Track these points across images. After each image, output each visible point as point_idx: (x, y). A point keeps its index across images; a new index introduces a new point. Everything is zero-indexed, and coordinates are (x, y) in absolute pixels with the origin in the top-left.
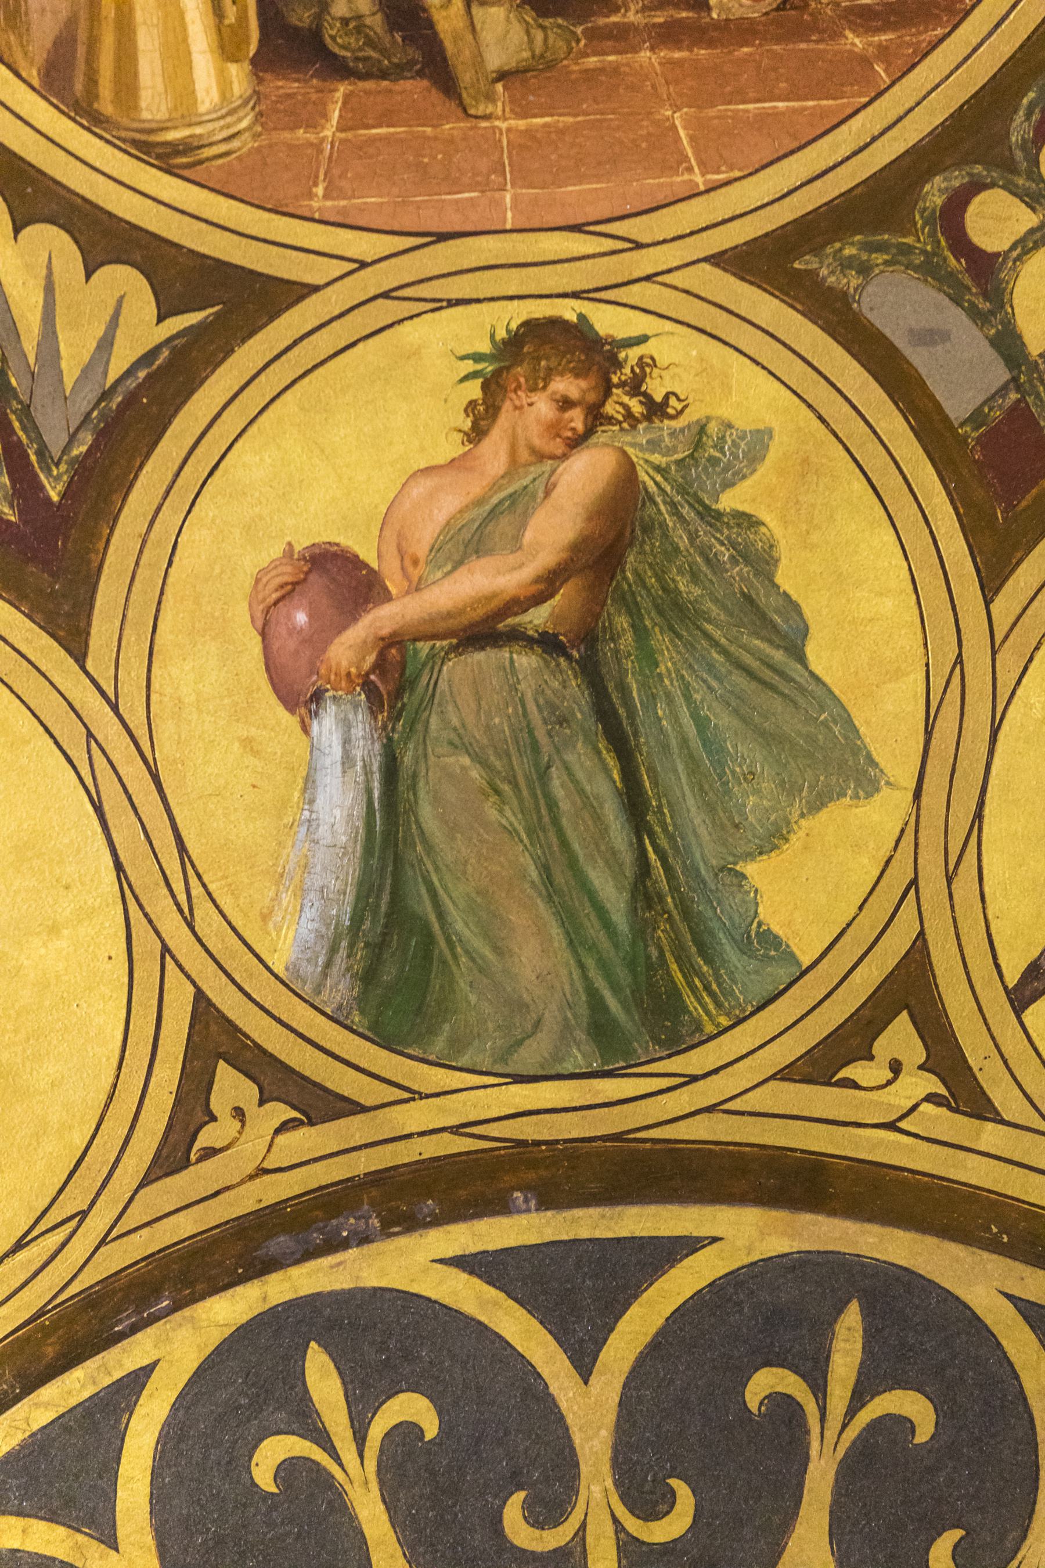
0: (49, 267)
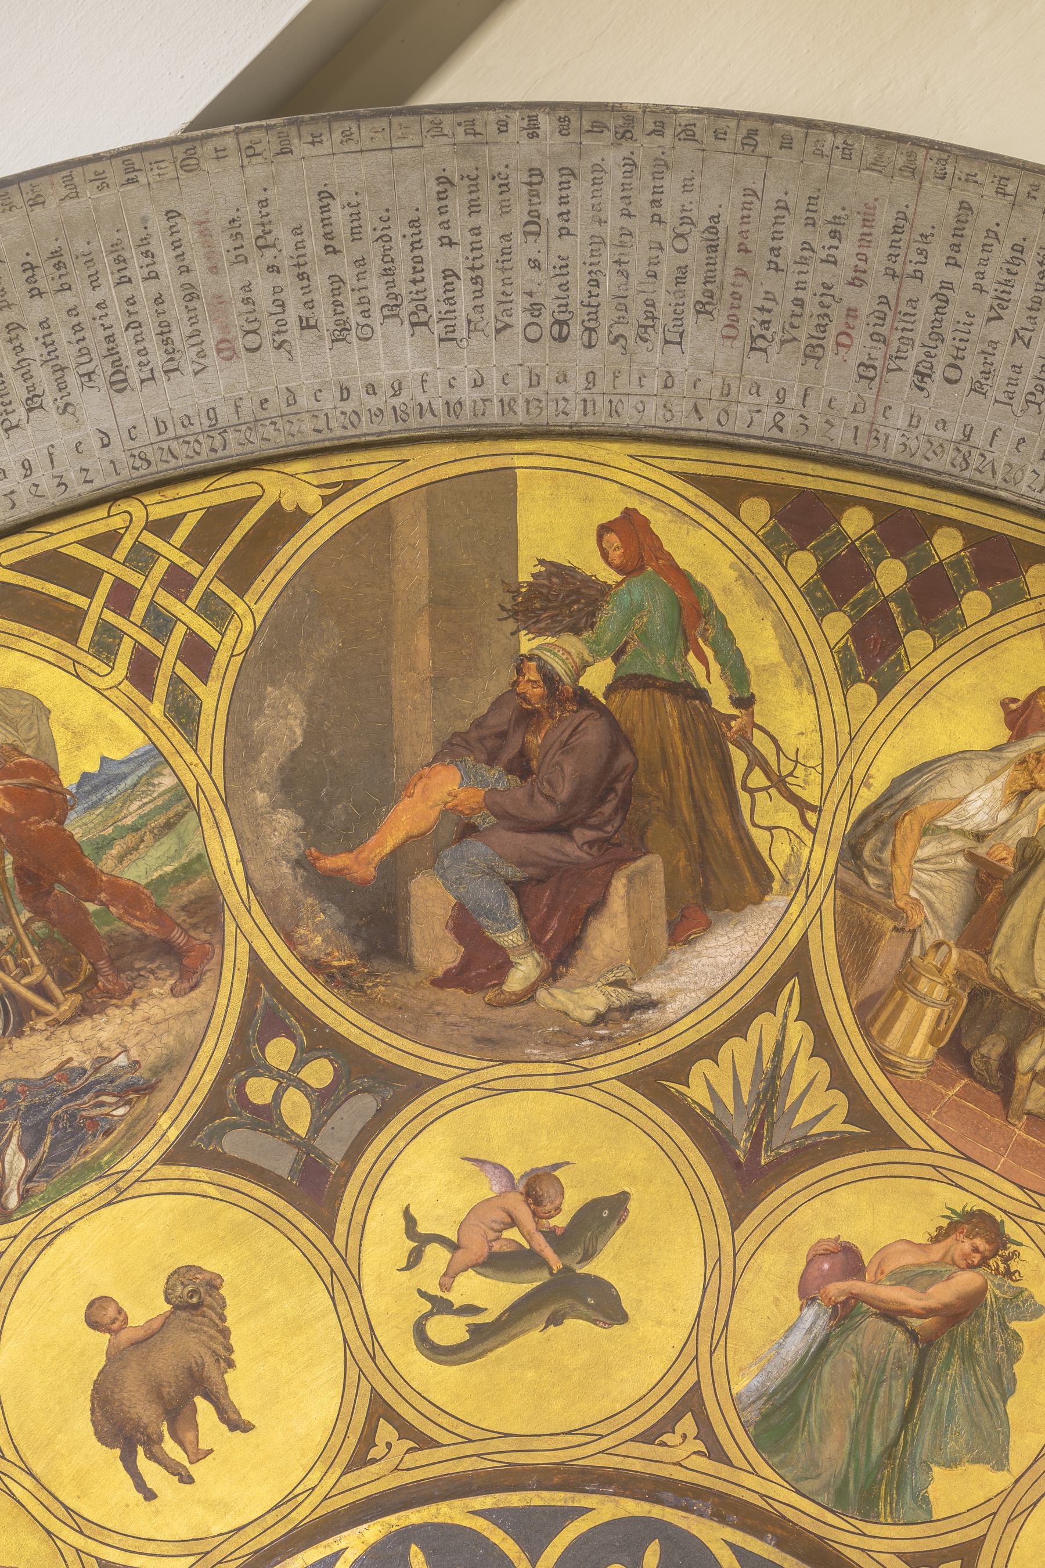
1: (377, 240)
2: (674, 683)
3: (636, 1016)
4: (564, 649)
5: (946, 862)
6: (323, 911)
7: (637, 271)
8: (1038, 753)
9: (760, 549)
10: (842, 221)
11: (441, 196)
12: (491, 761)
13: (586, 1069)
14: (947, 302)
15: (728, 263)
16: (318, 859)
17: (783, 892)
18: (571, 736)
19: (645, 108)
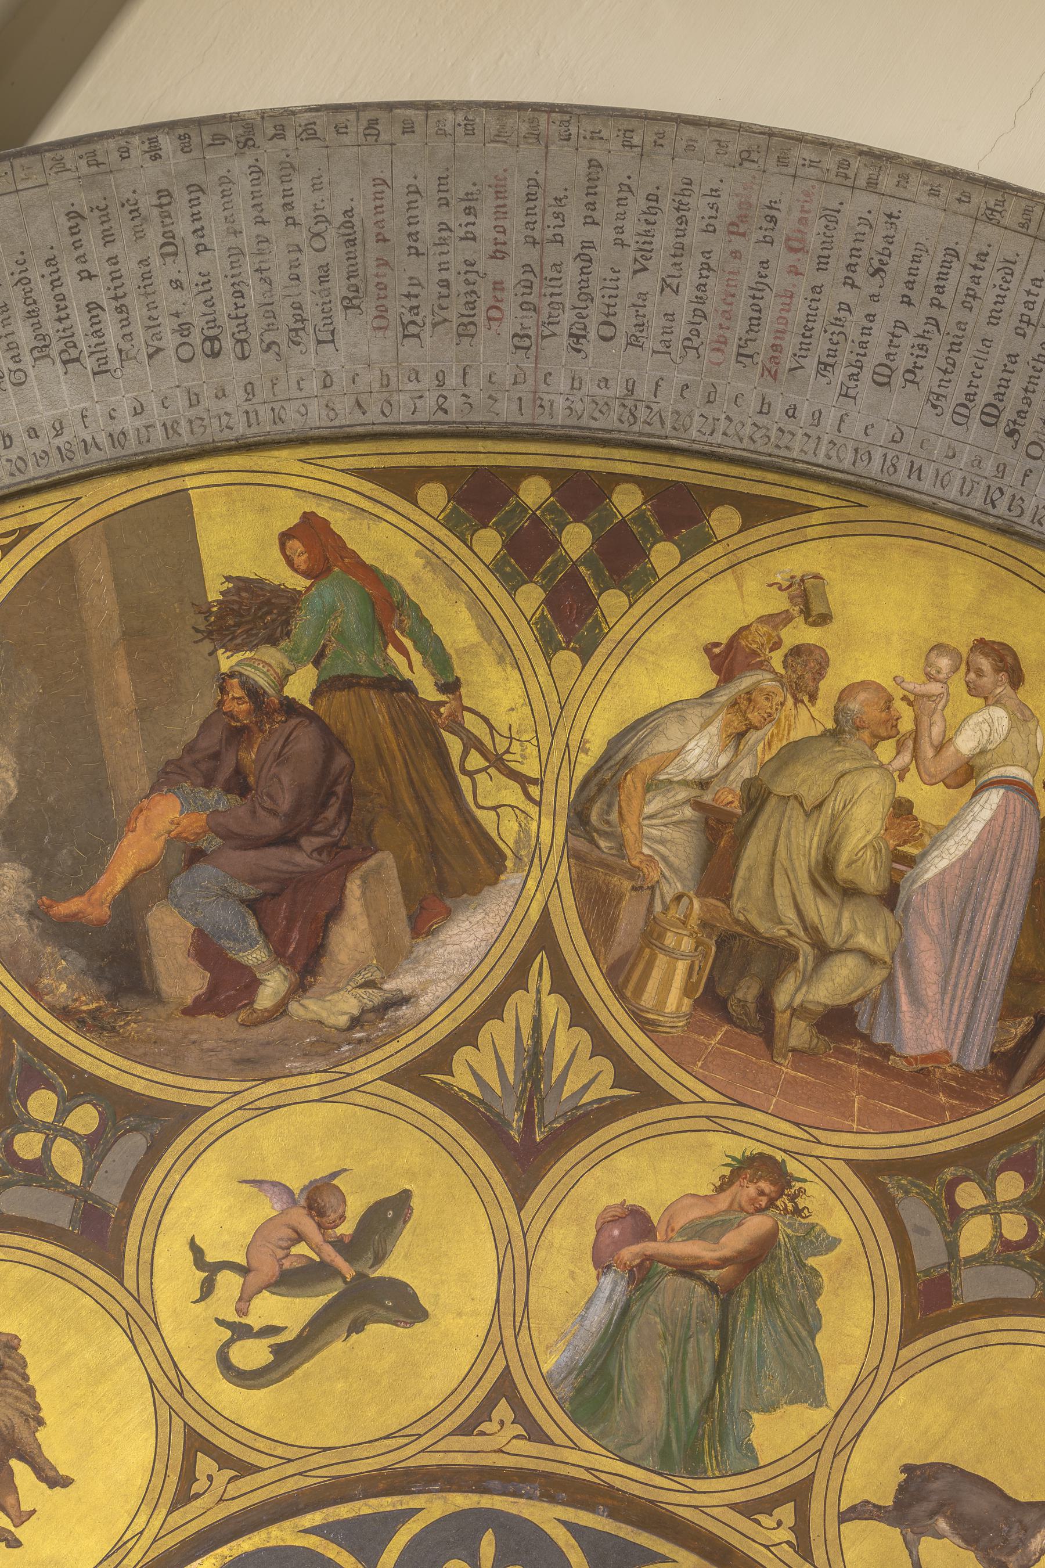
0: (577, 1047)
1: (16, 284)
2: (378, 679)
3: (391, 1014)
4: (263, 662)
5: (674, 815)
6: (64, 958)
7: (280, 277)
8: (748, 693)
9: (442, 533)
10: (475, 197)
11: (74, 231)
12: (208, 783)
13: (348, 1075)
14: (590, 261)
15: (368, 255)
16: (51, 907)
17: (518, 868)
18: (283, 746)
19: (263, 114)
